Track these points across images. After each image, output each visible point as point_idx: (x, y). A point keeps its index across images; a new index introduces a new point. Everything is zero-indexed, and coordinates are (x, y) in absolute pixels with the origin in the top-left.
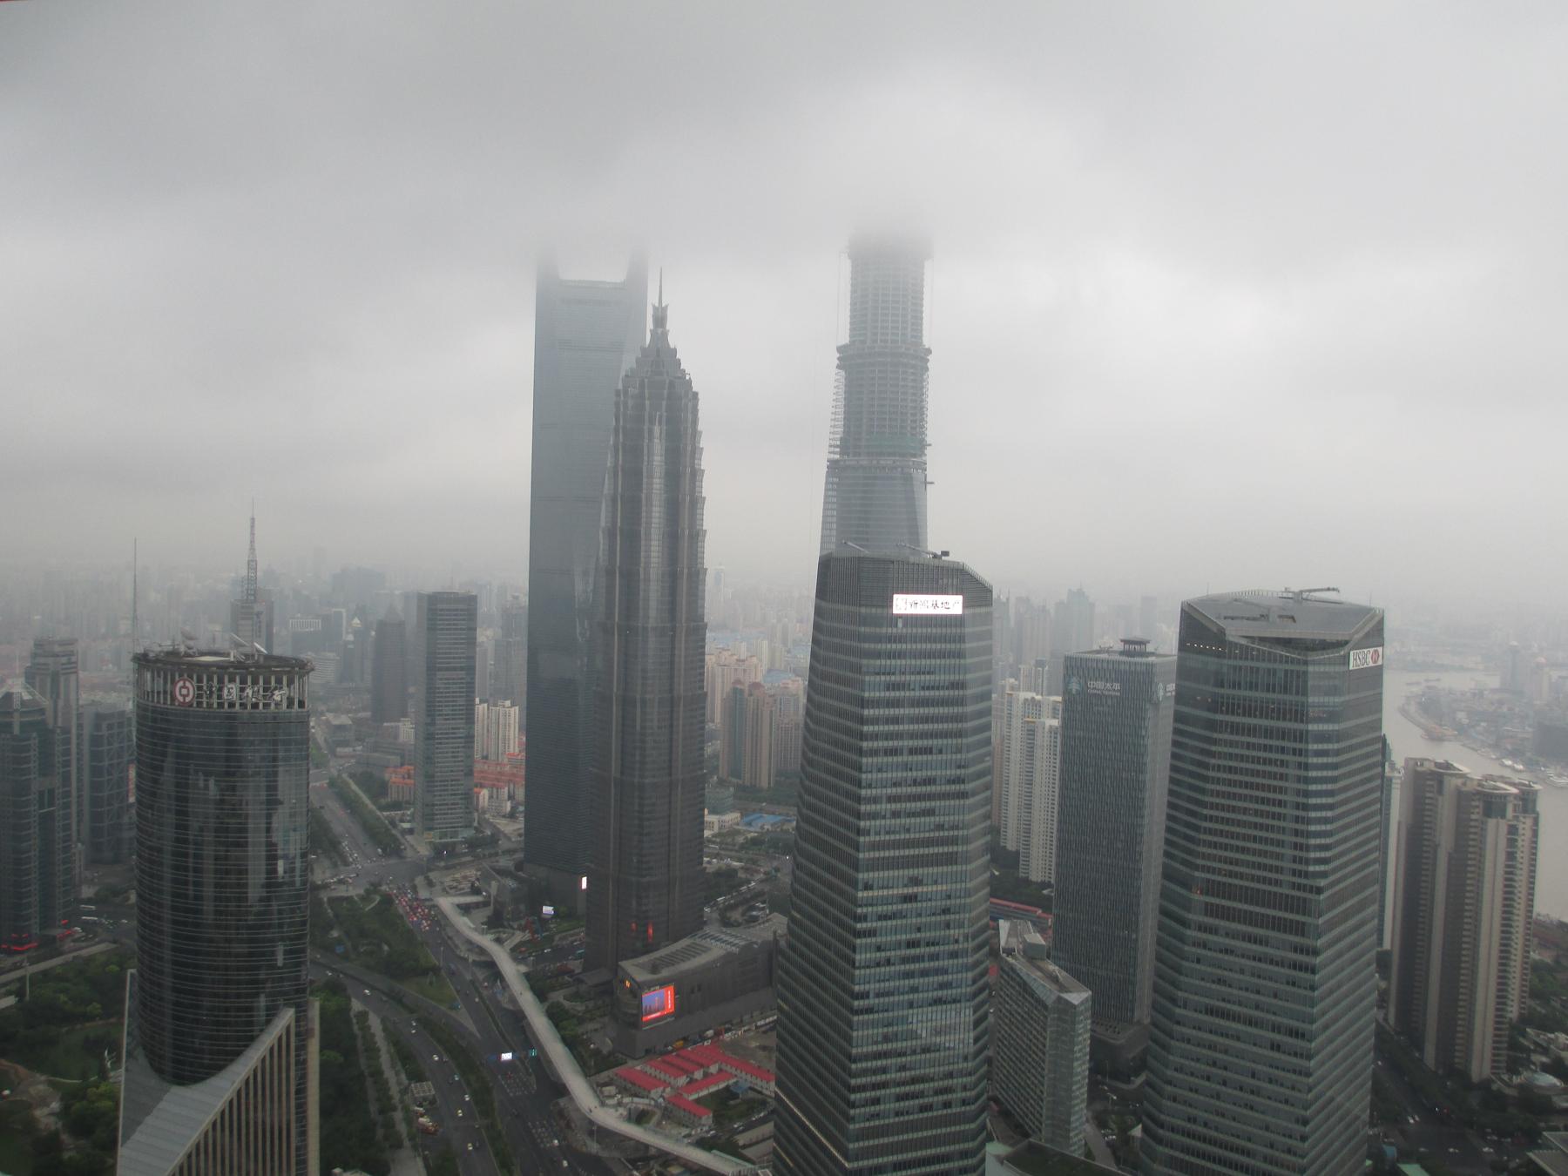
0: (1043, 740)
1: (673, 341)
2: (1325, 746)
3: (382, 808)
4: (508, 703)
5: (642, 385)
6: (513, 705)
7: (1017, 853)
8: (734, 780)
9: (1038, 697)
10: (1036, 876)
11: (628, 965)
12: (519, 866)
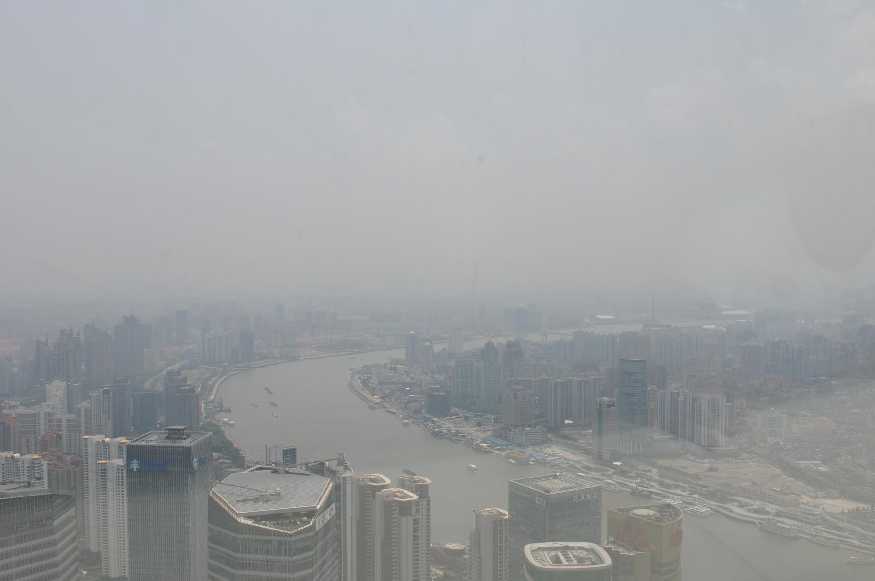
0: (111, 475)
7: (99, 553)
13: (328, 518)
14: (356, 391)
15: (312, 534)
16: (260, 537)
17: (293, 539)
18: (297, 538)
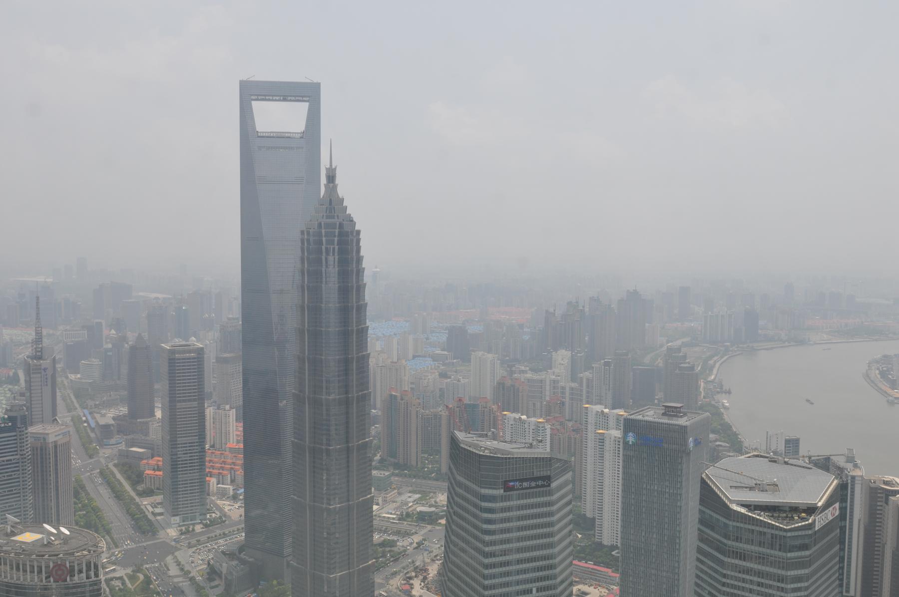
0: (609, 446)
1: (341, 192)
2: (799, 585)
3: (142, 494)
4: (227, 407)
5: (320, 225)
6: (231, 408)
7: (594, 519)
8: (392, 460)
9: (606, 411)
10: (606, 542)
12: (241, 549)
13: (830, 518)
14: (873, 382)
15: (810, 532)
16: (753, 528)
17: (789, 534)
18: (793, 534)
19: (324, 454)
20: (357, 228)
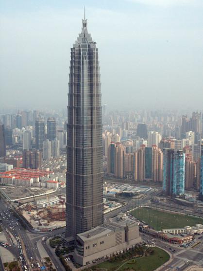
5: (80, 47)
8: (112, 174)
11: (78, 235)
19: (81, 151)
20: (97, 47)
